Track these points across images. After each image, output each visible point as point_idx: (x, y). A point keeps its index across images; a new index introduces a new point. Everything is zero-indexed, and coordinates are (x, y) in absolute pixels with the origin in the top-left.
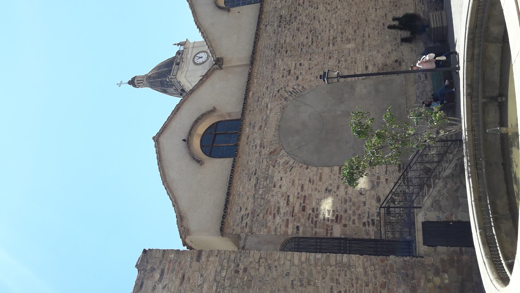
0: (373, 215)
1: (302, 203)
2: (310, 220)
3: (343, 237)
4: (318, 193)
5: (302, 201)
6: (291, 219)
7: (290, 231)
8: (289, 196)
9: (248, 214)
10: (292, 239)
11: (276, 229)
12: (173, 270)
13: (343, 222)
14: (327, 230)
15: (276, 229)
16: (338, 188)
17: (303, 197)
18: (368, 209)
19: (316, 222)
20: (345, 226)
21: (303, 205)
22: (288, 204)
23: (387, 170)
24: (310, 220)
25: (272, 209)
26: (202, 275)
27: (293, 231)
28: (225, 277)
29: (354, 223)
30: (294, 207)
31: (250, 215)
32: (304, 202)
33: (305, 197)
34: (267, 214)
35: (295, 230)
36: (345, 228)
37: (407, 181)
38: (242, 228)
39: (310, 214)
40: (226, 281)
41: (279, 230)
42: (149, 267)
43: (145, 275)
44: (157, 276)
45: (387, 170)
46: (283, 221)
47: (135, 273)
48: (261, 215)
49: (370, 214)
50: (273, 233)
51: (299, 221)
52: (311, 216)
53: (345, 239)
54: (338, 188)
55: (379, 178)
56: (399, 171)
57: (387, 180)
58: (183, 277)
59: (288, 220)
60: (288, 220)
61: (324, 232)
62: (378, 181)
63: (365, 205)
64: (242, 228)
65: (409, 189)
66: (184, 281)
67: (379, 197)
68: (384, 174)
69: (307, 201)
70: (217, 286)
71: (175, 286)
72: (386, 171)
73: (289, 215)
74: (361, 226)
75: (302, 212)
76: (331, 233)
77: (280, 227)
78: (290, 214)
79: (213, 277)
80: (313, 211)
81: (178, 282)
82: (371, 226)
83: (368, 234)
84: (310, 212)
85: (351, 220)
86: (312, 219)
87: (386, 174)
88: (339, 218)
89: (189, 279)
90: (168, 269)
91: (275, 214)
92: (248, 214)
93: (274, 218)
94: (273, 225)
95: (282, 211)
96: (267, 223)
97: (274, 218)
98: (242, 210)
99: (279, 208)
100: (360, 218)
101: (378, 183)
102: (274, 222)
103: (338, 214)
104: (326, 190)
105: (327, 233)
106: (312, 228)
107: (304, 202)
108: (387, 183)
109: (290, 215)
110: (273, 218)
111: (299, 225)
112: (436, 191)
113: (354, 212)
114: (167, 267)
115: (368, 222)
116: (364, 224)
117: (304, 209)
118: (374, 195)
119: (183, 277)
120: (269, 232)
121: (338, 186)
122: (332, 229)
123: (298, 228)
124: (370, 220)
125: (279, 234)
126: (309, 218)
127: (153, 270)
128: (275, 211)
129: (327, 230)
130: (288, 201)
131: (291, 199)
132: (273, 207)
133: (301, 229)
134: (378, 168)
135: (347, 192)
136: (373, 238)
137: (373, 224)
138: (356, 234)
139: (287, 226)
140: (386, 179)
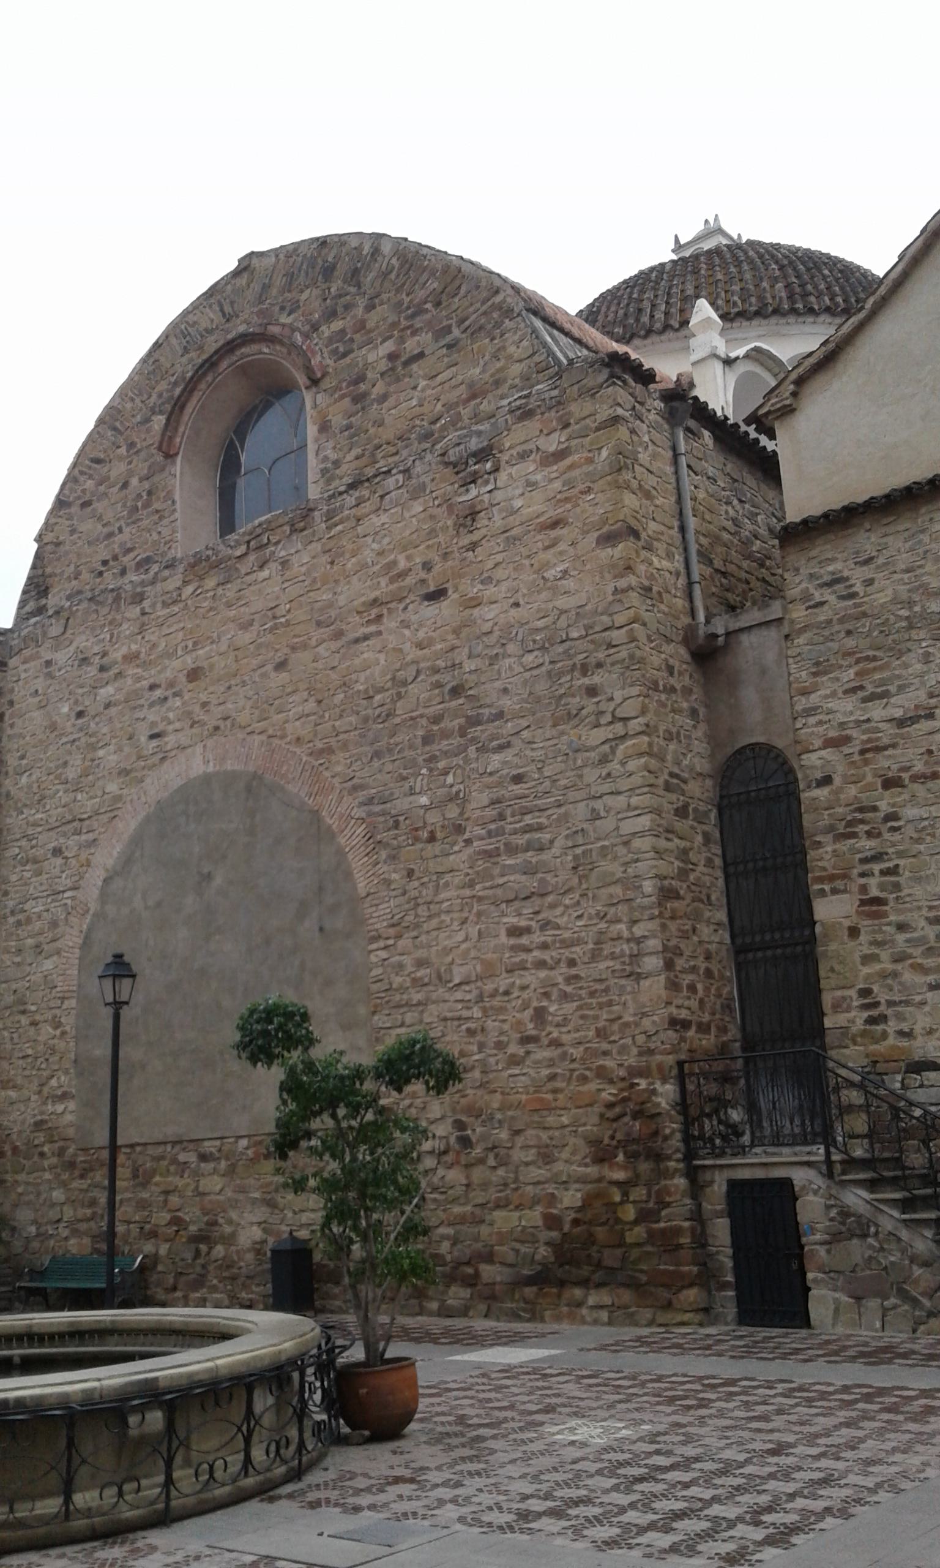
0: (900, 1017)
3: (818, 929)
5: (919, 767)
6: (854, 748)
7: (812, 759)
8: (931, 716)
9: (853, 595)
10: (791, 771)
11: (810, 712)
13: (865, 924)
14: (832, 878)
15: (810, 712)
22: (901, 723)
25: (877, 676)
27: (813, 767)
28: (568, 639)
31: (851, 603)
34: (858, 662)
35: (819, 775)
38: (806, 597)
39: (875, 809)
41: (812, 720)
46: (842, 725)
48: (850, 643)
50: (802, 703)
52: (870, 815)
53: (812, 939)
59: (847, 740)
60: (847, 740)
61: (824, 869)
64: (806, 597)
69: (919, 789)
73: (865, 737)
75: (879, 781)
77: (820, 723)
78: (869, 741)
82: (865, 1015)
83: (837, 1007)
91: (861, 688)
92: (853, 595)
93: (846, 692)
94: (826, 697)
95: (877, 712)
96: (826, 673)
97: (846, 692)
98: (865, 568)
99: (886, 695)
102: (834, 694)
103: (891, 904)
105: (820, 880)
106: (831, 829)
109: (864, 742)
110: (846, 686)
120: (805, 693)
122: (835, 891)
123: (827, 780)
124: (882, 1008)
125: (798, 725)
128: (870, 689)
129: (832, 878)
130: (914, 720)
131: (925, 726)
132: (885, 674)
133: (823, 793)
136: (828, 1023)
137: (872, 1021)
139: (831, 743)
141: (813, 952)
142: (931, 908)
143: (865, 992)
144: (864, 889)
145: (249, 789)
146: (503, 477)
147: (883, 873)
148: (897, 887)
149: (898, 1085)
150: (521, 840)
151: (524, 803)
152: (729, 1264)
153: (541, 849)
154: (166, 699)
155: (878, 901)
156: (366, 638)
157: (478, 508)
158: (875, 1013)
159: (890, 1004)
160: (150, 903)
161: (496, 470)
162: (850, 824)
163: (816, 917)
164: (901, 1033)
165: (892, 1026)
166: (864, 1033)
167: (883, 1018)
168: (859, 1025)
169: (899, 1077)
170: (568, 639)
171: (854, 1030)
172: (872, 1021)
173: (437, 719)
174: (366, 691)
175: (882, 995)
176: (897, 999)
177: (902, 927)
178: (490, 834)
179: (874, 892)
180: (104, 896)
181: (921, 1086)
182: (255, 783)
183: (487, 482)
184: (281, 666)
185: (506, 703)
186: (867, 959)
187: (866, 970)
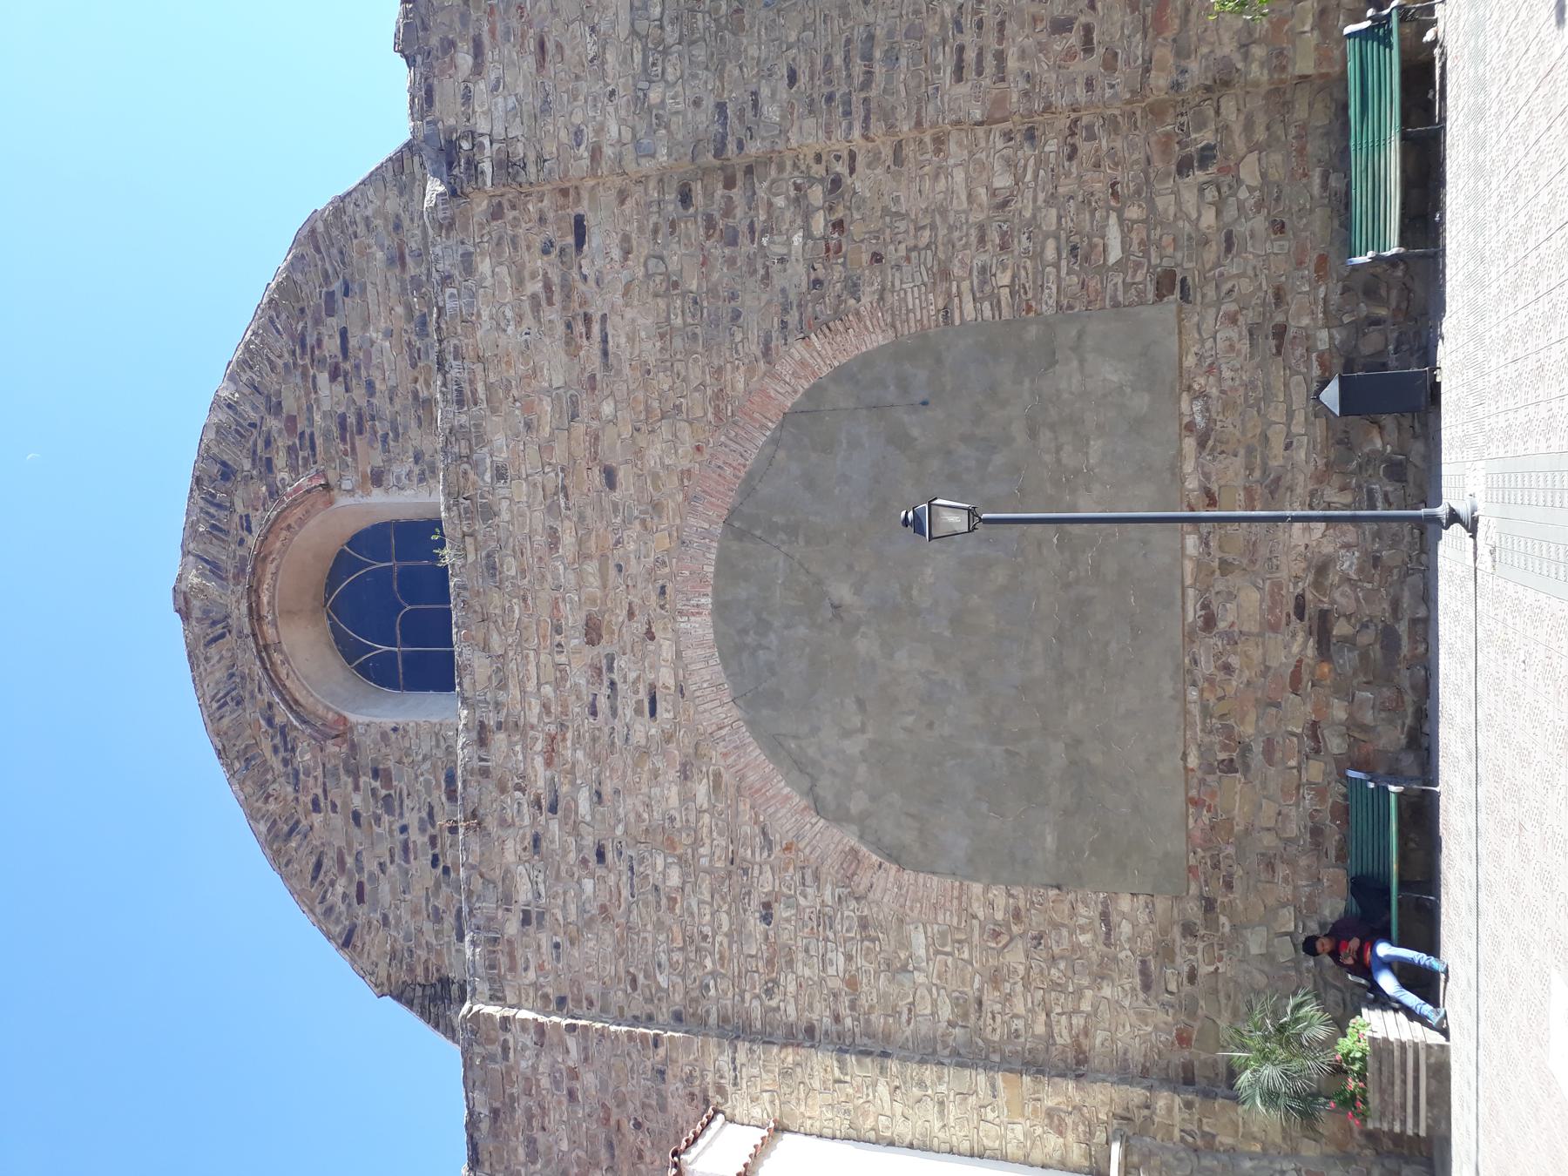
12: (507, 33)
26: (593, 29)
28: (661, 20)
40: (668, 28)
42: (434, 41)
43: (431, 66)
44: (465, 60)
47: (399, 75)
58: (542, 46)
66: (548, 59)
70: (645, 49)
71: (524, 77)
79: (628, 25)
81: (529, 63)
89: (559, 47)
90: (492, 32)
114: (486, 28)
119: (542, 46)
127: (449, 45)
145: (741, 535)
146: (482, 126)
150: (858, 68)
151: (819, 66)
153: (871, 37)
154: (613, 684)
156: (605, 340)
157: (503, 156)
160: (857, 721)
161: (472, 135)
170: (661, 20)
173: (710, 223)
174: (662, 336)
178: (847, 113)
180: (838, 816)
182: (737, 524)
183: (482, 145)
184: (610, 477)
185: (709, 102)
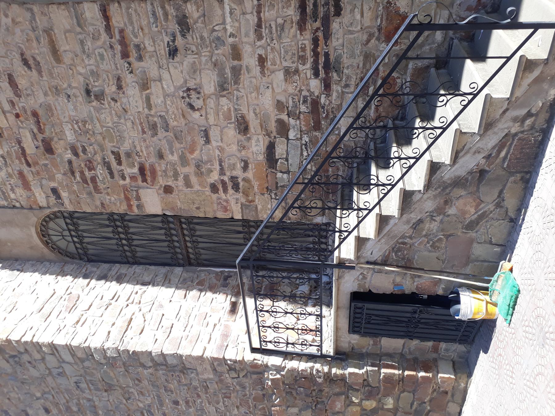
1: (35, 130)
2: (78, 175)
4: (69, 101)
13: (162, 181)
16: (120, 87)
17: (29, 113)
18: (217, 152)
19: (93, 179)
20: (168, 190)
21: (40, 137)
23: (260, 19)
24: (78, 175)
29: (188, 184)
30: (19, 142)
32: (40, 130)
33: (35, 114)
36: (169, 195)
37: (327, 66)
45: (260, 19)
49: (226, 166)
51: (52, 178)
52: (75, 165)
54: (120, 87)
55: (236, 54)
56: (302, 25)
57: (262, 60)
62: (236, 63)
63: (208, 141)
65: (328, 95)
67: (243, 117)
68: (252, 35)
72: (259, 25)
74: (208, 190)
76: (139, 207)
80: (76, 154)
84: (69, 155)
85: (181, 178)
86: (82, 173)
87: (260, 37)
88: (148, 173)
100: (202, 173)
101: (236, 72)
104: (88, 92)
107: (40, 130)
108: (262, 73)
111: (53, 184)
112: (408, 222)
113: (184, 161)
115: (224, 183)
116: (214, 188)
117: (49, 150)
118: (229, 110)
121: (119, 79)
126: (73, 173)
133: (64, 194)
134: (231, 13)
135: (148, 99)
138: (198, 208)
140: (260, 56)
141: (187, 218)
142: (144, 132)
143: (214, 188)
144: (133, 178)
147: (120, 163)
148: (128, 155)
149: (285, 176)
152: (415, 343)
155: (142, 170)
158: (230, 185)
159: (222, 172)
162: (85, 181)
163: (160, 213)
164: (245, 168)
165: (238, 172)
166: (246, 194)
167: (234, 179)
168: (240, 195)
169: (279, 175)
171: (243, 200)
172: (236, 187)
175: (215, 177)
176: (218, 168)
177: (161, 156)
179: (136, 170)
181: (287, 160)
186: (188, 184)
187: (197, 187)
